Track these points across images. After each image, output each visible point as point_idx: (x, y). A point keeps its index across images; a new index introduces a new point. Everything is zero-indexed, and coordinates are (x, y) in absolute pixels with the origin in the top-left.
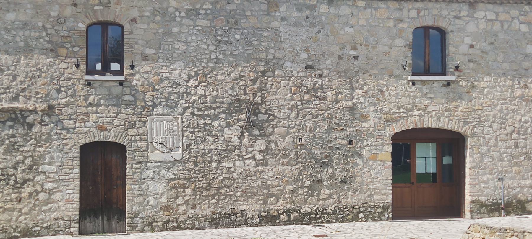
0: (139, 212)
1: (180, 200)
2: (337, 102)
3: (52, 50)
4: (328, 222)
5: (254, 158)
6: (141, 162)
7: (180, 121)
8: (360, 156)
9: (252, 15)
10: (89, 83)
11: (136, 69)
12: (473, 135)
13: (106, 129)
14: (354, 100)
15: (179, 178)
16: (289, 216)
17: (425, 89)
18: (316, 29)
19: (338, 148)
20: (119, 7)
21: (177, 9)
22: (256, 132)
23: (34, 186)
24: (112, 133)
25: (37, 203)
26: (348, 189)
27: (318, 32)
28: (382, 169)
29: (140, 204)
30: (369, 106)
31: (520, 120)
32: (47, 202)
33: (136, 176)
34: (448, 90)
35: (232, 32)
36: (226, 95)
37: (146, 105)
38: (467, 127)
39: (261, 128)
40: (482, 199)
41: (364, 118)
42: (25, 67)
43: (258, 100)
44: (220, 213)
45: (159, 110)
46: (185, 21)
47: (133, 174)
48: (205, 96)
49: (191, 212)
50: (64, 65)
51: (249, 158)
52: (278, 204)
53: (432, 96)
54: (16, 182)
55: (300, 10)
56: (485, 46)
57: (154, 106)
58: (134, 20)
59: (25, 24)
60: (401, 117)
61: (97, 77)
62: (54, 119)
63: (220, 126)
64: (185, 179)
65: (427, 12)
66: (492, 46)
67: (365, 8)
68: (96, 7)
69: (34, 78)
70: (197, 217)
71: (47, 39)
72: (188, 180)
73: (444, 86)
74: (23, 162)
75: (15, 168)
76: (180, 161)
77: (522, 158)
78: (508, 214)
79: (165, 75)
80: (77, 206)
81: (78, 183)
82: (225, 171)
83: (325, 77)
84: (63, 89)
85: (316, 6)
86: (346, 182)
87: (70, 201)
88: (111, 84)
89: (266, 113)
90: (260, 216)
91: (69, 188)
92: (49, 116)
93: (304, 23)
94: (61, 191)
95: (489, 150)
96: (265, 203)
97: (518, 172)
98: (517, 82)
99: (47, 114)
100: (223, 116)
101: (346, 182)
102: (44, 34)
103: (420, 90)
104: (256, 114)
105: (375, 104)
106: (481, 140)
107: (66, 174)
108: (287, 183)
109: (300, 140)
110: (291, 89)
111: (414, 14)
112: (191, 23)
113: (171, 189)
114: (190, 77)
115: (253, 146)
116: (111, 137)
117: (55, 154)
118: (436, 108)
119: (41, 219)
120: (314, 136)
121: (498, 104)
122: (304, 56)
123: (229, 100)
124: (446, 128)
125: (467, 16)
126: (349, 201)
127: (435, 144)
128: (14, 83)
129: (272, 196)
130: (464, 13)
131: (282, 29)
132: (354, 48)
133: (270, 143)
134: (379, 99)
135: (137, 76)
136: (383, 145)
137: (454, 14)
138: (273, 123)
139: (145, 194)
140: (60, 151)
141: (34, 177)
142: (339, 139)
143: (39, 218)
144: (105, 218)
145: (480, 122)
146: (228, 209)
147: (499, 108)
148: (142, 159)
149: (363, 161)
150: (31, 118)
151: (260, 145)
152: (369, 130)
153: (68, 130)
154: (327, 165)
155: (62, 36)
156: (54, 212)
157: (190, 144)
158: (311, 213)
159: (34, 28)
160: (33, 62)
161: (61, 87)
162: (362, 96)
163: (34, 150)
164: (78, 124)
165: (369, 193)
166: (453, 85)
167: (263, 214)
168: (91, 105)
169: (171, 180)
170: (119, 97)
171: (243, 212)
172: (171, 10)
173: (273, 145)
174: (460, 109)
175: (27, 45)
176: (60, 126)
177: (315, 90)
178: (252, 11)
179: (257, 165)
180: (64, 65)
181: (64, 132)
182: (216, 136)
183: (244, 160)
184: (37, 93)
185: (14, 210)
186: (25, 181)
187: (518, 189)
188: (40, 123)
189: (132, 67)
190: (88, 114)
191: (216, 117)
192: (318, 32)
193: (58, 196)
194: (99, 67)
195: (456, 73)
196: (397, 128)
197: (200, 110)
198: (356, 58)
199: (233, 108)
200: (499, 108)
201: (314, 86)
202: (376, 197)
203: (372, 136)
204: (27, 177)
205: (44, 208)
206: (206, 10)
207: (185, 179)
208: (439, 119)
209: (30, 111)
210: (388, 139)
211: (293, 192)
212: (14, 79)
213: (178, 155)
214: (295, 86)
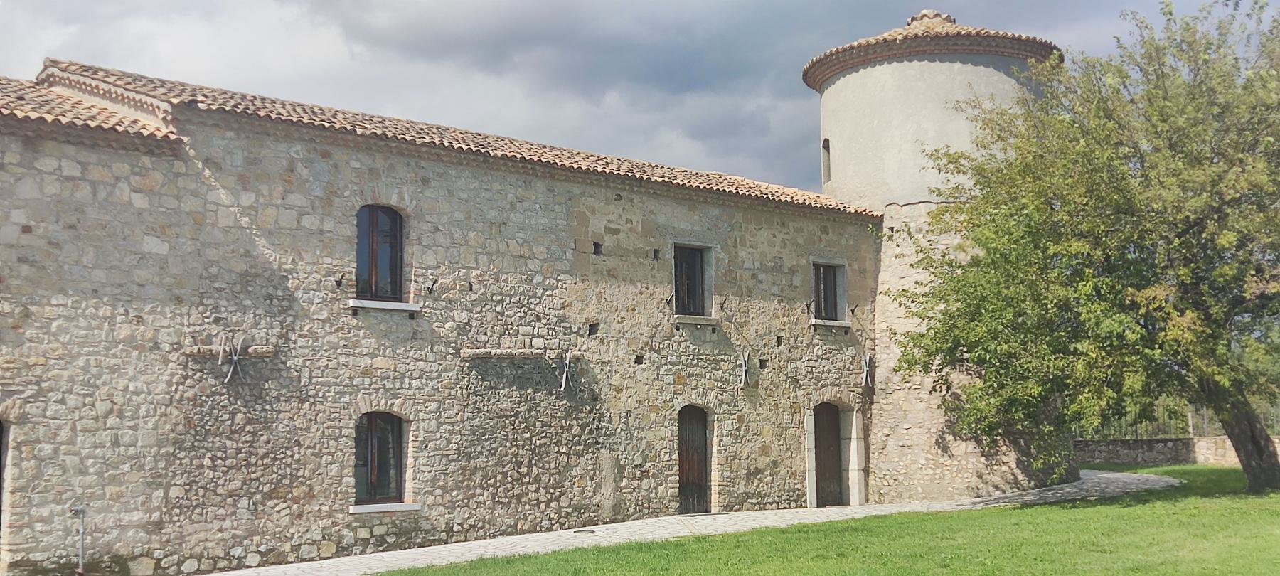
12: (23, 419)
31: (126, 389)
38: (9, 402)
40: (37, 557)
56: (56, 230)
66: (72, 232)
77: (126, 467)
95: (56, 451)
97: (117, 497)
98: (122, 310)
106: (41, 430)
121: (79, 355)
125: (19, 165)
145: (40, 391)
147: (81, 362)
187: (116, 533)
200: (81, 362)
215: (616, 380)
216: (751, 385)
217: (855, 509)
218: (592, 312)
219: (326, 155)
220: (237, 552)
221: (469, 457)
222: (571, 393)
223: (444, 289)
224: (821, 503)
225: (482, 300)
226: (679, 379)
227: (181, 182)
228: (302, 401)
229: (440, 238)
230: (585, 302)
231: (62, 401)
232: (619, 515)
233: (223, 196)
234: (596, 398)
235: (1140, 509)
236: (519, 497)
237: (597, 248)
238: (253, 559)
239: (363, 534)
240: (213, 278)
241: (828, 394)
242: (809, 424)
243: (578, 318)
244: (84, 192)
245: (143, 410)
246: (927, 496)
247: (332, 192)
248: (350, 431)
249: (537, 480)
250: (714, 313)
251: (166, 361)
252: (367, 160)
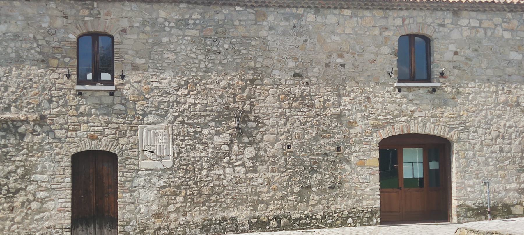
0: (131, 220)
1: (171, 208)
2: (325, 109)
3: (43, 61)
4: (318, 227)
5: (243, 165)
6: (132, 171)
7: (170, 130)
8: (348, 162)
9: (240, 25)
10: (80, 93)
11: (127, 79)
12: (459, 140)
13: (97, 138)
14: (342, 107)
15: (170, 186)
16: (279, 223)
17: (411, 96)
18: (303, 38)
19: (326, 155)
20: (109, 18)
21: (166, 20)
22: (246, 140)
23: (26, 195)
24: (103, 142)
25: (29, 212)
26: (337, 195)
27: (306, 41)
28: (370, 174)
29: (131, 212)
30: (356, 113)
32: (39, 211)
33: (127, 184)
34: (433, 96)
35: (221, 41)
36: (215, 103)
37: (137, 114)
38: (453, 132)
39: (250, 135)
40: (469, 203)
41: (352, 124)
42: (17, 78)
43: (247, 107)
44: (210, 220)
45: (150, 118)
46: (174, 31)
47: (125, 182)
48: (195, 105)
49: (182, 219)
50: (55, 76)
51: (239, 166)
52: (268, 210)
53: (418, 102)
54: (8, 191)
55: (287, 19)
56: (469, 52)
57: (145, 115)
58: (124, 31)
59: (16, 36)
60: (389, 124)
61: (88, 87)
62: (46, 128)
63: (210, 134)
64: (175, 186)
65: (411, 20)
66: (476, 53)
67: (351, 17)
68: (86, 19)
69: (26, 89)
70: (188, 224)
71: (38, 50)
72: (179, 187)
73: (430, 92)
74: (15, 172)
75: (7, 178)
76: (170, 169)
77: (507, 162)
78: (494, 217)
79: (155, 84)
80: (69, 214)
81: (70, 192)
82: (215, 178)
83: (313, 85)
84: (54, 99)
85: (303, 15)
86: (335, 188)
87: (62, 210)
88: (102, 93)
89: (255, 121)
90: (250, 223)
91: (63, 196)
92: (41, 126)
93: (291, 32)
94: (53, 200)
95: (474, 155)
96: (255, 209)
97: (504, 177)
98: (501, 88)
99: (39, 124)
100: (212, 124)
101: (335, 188)
102: (35, 45)
103: (406, 97)
104: (245, 122)
105: (362, 111)
106: (467, 145)
107: (58, 183)
108: (276, 189)
109: (289, 147)
110: (279, 97)
111: (399, 22)
112: (181, 33)
113: (162, 197)
114: (179, 86)
115: (243, 153)
116: (102, 145)
117: (47, 164)
118: (422, 114)
119: (34, 228)
120: (303, 143)
121: (482, 110)
122: (292, 64)
123: (218, 109)
124: (432, 133)
125: (452, 24)
126: (338, 206)
127: (421, 150)
128: (6, 94)
129: (262, 202)
130: (448, 21)
131: (269, 38)
132: (341, 56)
133: (259, 150)
134: (366, 106)
135: (127, 86)
136: (371, 151)
137: (438, 21)
138: (262, 130)
139: (136, 202)
140: (52, 161)
141: (26, 186)
143: (31, 227)
144: (97, 226)
145: (466, 127)
146: (219, 217)
147: (483, 113)
148: (133, 167)
149: (351, 167)
150: (22, 129)
151: (250, 152)
152: (356, 136)
153: (59, 139)
154: (316, 171)
155: (53, 47)
156: (47, 220)
157: (181, 153)
158: (300, 219)
159: (25, 39)
160: (24, 73)
161: (52, 97)
162: (349, 103)
163: (26, 160)
164: (69, 134)
165: (357, 198)
166: (438, 92)
167: (253, 221)
168: (82, 114)
169: (162, 187)
170: (110, 106)
171: (233, 219)
172: (160, 20)
173: (262, 152)
174: (446, 114)
175: (19, 56)
176: (51, 135)
177: (303, 98)
178: (240, 21)
179: (247, 172)
180: (55, 76)
181: (55, 141)
182: (206, 143)
183: (234, 167)
184: (29, 103)
185: (6, 219)
186: (18, 191)
187: (504, 193)
188: (32, 133)
189: (123, 77)
190: (79, 124)
191: (206, 125)
192: (306, 41)
193: (50, 205)
194: (89, 77)
195: (441, 80)
196: (384, 134)
197: (189, 118)
198: (343, 65)
199: (223, 116)
200: (483, 113)
201: (302, 93)
202: (364, 203)
203: (359, 142)
204: (19, 186)
205: (37, 217)
206: (195, 20)
207: (175, 186)
208: (425, 125)
209: (22, 121)
210: (375, 145)
211: (282, 198)
212: (6, 90)
213: (168, 163)
214: (284, 93)
231: (476, 132)
244: (481, 32)
245: (514, 135)
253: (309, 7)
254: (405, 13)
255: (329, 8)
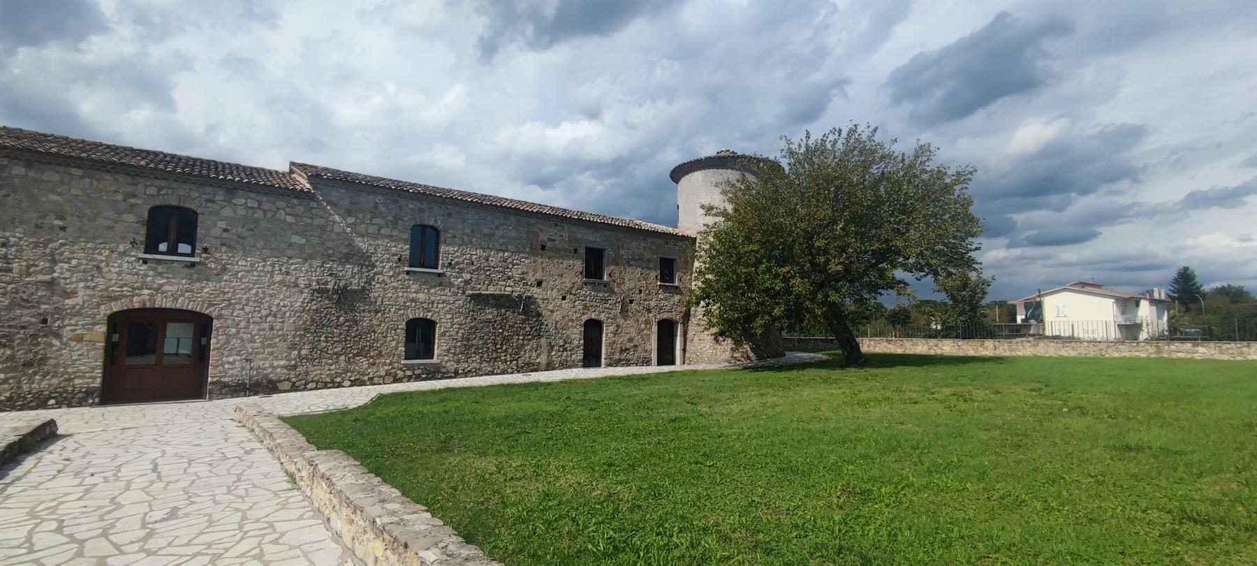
2: (29, 274)
8: (58, 336)
12: (220, 317)
14: (55, 275)
17: (160, 269)
19: (24, 327)
26: (35, 373)
27: (7, 196)
34: (191, 271)
40: (226, 380)
65: (170, 191)
67: (82, 177)
78: (256, 394)
95: (238, 332)
97: (272, 353)
103: (153, 269)
105: (87, 280)
106: (230, 322)
127: (191, 325)
132: (62, 218)
142: (27, 316)
145: (230, 304)
147: (254, 291)
192: (7, 196)
196: (116, 307)
198: (63, 229)
200: (254, 291)
203: (78, 314)
215: (550, 307)
216: (624, 312)
217: (678, 367)
218: (539, 276)
219: (395, 201)
220: (339, 380)
221: (468, 340)
222: (525, 312)
223: (457, 263)
224: (659, 364)
225: (478, 269)
226: (585, 307)
227: (314, 211)
228: (377, 312)
229: (456, 240)
230: (535, 272)
231: (242, 309)
232: (550, 367)
233: (337, 218)
234: (539, 315)
235: (783, 375)
236: (495, 359)
237: (543, 247)
238: (347, 383)
239: (409, 373)
240: (330, 256)
241: (665, 316)
242: (655, 328)
243: (531, 278)
244: (259, 214)
246: (710, 362)
247: (397, 219)
248: (403, 325)
249: (506, 351)
250: (605, 278)
251: (302, 292)
252: (419, 205)
253: (16, 158)
254: (163, 183)
255: (49, 163)
